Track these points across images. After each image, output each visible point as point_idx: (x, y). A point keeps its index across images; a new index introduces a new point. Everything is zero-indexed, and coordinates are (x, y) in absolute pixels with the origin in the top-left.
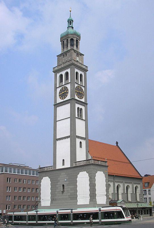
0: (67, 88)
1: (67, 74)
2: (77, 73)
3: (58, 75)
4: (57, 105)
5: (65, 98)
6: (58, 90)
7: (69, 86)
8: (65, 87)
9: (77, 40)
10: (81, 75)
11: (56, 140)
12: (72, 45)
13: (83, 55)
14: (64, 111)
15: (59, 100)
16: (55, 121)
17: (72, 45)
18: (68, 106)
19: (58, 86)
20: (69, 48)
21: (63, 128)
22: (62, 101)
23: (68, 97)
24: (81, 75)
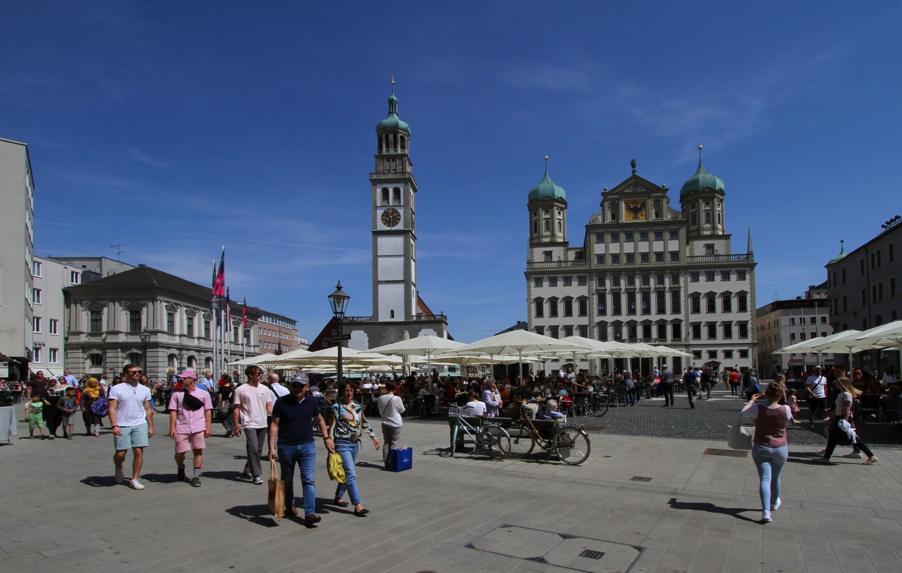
1: (397, 191)
4: (377, 233)
5: (394, 226)
6: (380, 212)
7: (401, 211)
11: (376, 283)
14: (391, 245)
15: (381, 226)
16: (376, 257)
18: (400, 240)
19: (379, 204)
21: (390, 267)
22: (389, 229)
23: (400, 226)
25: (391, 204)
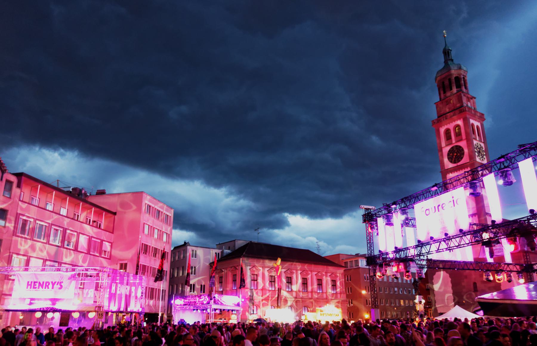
0: (460, 147)
2: (473, 125)
3: (442, 130)
7: (463, 144)
8: (457, 146)
9: (464, 78)
10: (477, 127)
12: (459, 86)
13: (475, 98)
17: (459, 86)
20: (455, 90)
23: (465, 160)
24: (477, 127)
25: (454, 142)
